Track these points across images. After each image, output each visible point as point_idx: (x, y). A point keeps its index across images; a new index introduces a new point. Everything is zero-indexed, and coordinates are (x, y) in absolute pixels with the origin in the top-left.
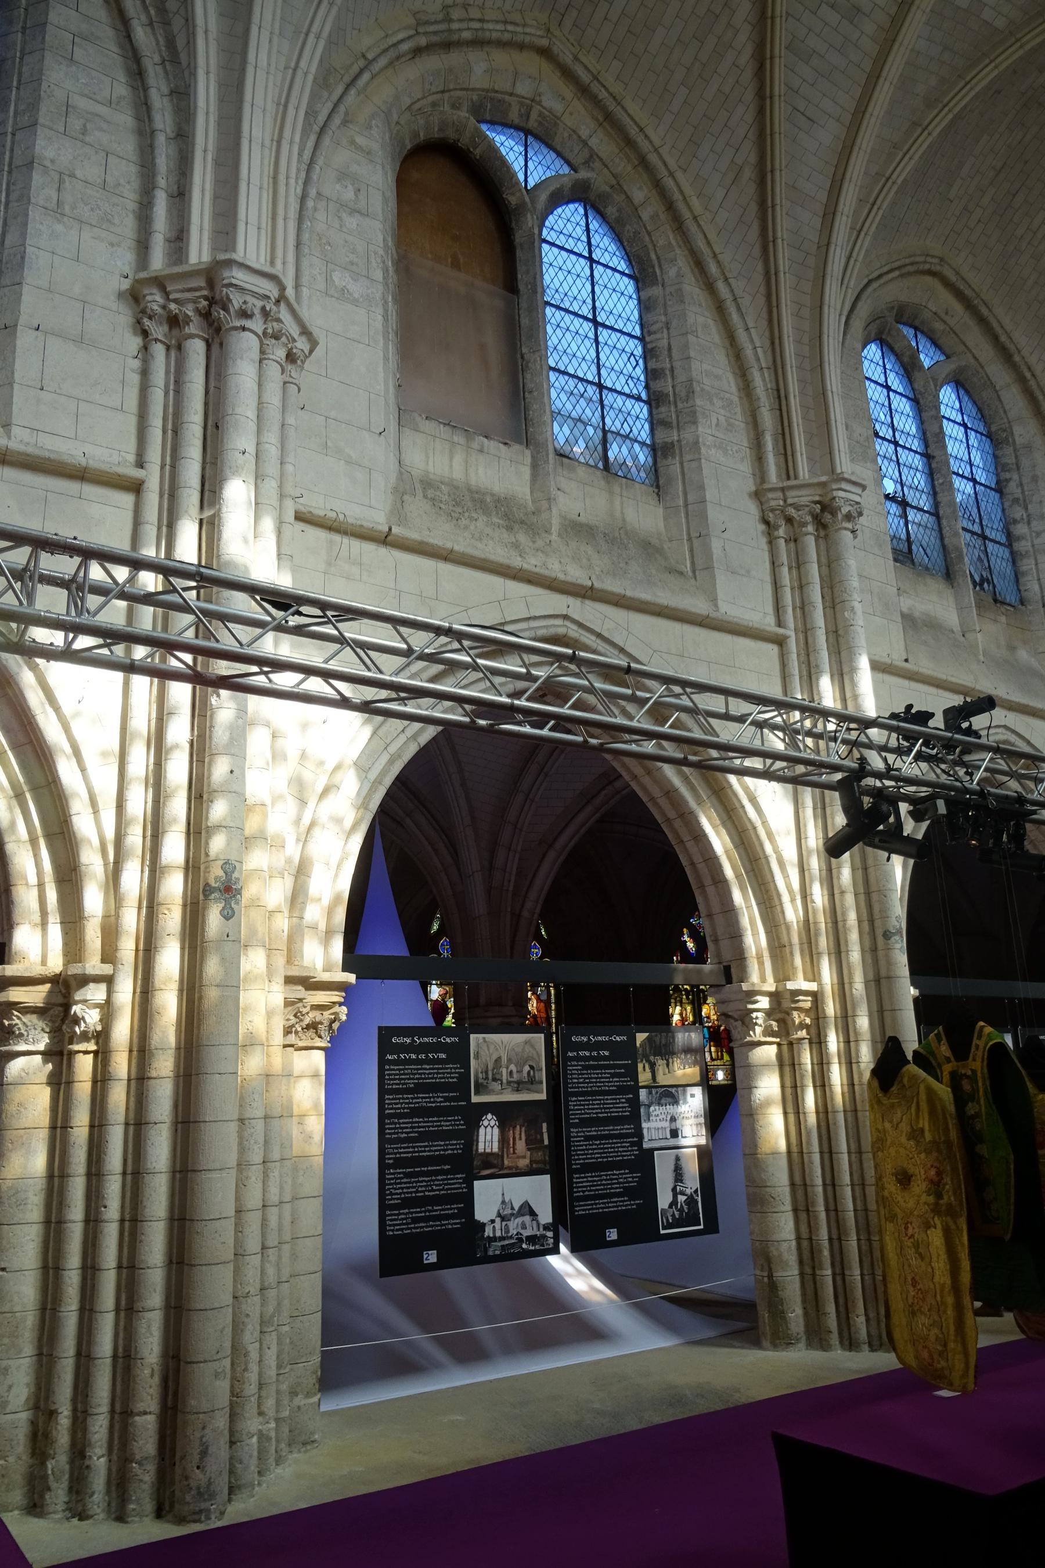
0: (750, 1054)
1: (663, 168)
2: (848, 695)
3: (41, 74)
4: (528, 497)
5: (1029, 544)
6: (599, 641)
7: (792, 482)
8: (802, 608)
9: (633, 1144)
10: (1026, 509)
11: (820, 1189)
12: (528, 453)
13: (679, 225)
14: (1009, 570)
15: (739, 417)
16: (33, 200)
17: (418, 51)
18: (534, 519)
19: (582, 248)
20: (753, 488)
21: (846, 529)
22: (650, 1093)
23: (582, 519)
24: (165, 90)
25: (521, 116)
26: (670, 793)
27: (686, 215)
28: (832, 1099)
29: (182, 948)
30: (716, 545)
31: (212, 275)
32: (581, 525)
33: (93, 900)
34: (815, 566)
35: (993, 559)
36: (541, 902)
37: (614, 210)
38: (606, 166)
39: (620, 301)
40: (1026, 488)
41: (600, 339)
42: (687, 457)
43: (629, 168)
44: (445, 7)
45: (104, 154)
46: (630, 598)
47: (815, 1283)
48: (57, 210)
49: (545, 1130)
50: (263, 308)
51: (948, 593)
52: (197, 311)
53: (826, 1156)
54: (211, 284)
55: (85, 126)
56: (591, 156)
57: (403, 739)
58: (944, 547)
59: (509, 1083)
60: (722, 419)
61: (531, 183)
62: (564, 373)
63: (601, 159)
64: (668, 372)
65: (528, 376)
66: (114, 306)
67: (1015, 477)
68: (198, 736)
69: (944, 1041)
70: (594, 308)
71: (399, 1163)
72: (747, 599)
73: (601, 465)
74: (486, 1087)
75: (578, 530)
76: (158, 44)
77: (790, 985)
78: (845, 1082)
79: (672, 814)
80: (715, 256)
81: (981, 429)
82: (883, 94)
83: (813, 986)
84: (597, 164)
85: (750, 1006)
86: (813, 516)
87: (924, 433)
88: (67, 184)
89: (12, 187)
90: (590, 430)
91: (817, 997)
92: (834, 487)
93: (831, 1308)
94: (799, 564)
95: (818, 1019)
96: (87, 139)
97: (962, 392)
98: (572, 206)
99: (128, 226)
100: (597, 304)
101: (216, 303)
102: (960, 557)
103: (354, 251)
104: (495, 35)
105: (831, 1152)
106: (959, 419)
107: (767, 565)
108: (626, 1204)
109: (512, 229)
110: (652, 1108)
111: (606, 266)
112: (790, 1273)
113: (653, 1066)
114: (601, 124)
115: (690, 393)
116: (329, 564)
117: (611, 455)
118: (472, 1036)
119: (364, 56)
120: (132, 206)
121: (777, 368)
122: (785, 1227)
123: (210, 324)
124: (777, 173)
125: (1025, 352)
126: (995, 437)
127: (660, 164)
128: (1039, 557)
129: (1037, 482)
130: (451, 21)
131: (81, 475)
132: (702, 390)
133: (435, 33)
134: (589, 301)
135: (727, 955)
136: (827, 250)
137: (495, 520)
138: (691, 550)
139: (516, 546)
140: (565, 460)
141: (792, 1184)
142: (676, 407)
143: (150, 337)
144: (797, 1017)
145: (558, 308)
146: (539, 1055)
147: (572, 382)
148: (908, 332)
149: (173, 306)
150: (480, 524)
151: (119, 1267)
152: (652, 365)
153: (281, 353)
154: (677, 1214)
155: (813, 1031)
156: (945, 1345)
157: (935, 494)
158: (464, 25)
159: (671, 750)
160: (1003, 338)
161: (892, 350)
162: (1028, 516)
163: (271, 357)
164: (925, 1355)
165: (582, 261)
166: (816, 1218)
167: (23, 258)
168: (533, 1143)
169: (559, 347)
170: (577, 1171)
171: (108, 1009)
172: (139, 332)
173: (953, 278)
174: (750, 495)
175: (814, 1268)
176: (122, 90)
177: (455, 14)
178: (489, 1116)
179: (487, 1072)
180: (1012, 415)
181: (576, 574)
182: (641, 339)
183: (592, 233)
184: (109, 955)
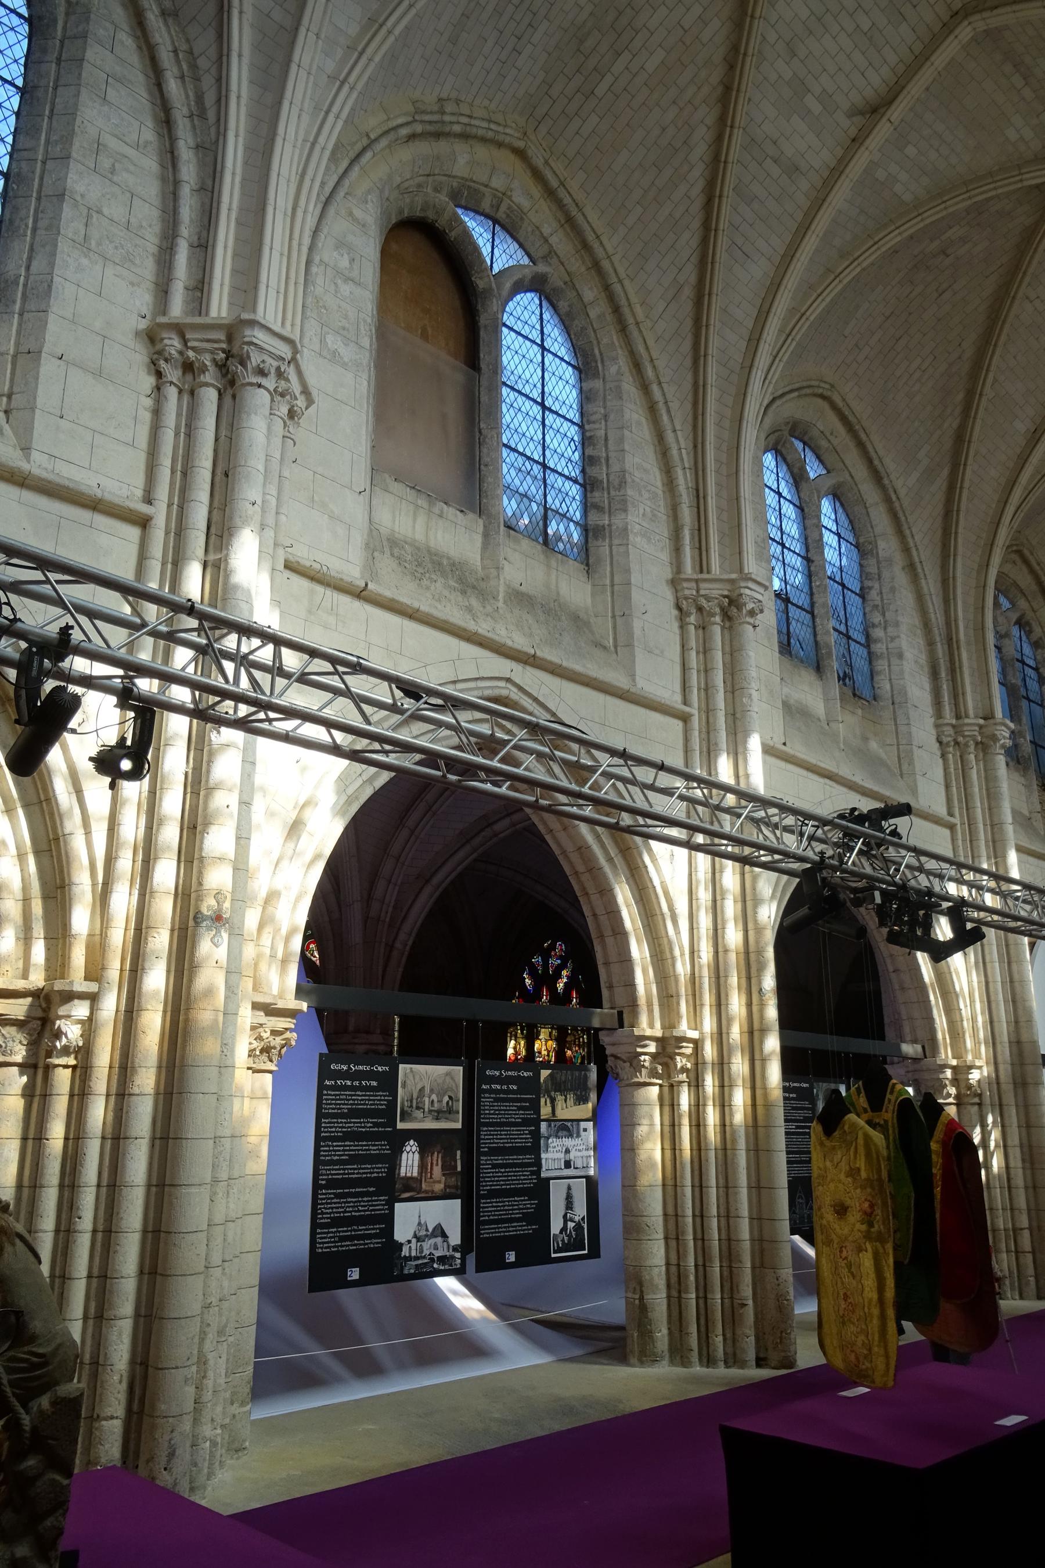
0: (635, 1093)
1: (613, 275)
2: (741, 773)
3: (77, 109)
4: (479, 564)
6: (534, 704)
7: (705, 576)
8: (706, 690)
9: (532, 1173)
10: (884, 615)
11: (690, 1220)
12: (481, 522)
13: (623, 329)
14: (866, 668)
15: (662, 509)
16: (62, 231)
17: (412, 137)
18: (483, 585)
19: (535, 335)
20: (670, 576)
21: (749, 623)
22: (550, 1126)
23: (523, 589)
24: (191, 142)
25: (492, 206)
26: (583, 849)
27: (631, 320)
28: (706, 1137)
29: (168, 971)
30: (637, 625)
31: (232, 331)
32: (523, 594)
33: (81, 919)
34: (720, 653)
35: (854, 657)
36: (414, 935)
37: (566, 304)
38: (562, 264)
41: (547, 422)
42: (616, 542)
43: (583, 269)
44: (440, 100)
45: (129, 195)
46: (565, 668)
47: (680, 1306)
48: (84, 244)
49: (458, 1157)
50: (278, 369)
51: (818, 684)
52: (214, 360)
53: (697, 1190)
54: (230, 339)
55: (113, 165)
56: (550, 252)
57: (360, 782)
58: (816, 642)
59: (430, 1111)
60: (648, 509)
61: (496, 269)
62: (515, 450)
63: (558, 257)
64: (603, 461)
65: (485, 450)
66: (131, 344)
67: (877, 586)
68: (194, 769)
69: (863, 1094)
70: (543, 392)
71: (332, 1184)
72: (659, 675)
73: (541, 540)
74: (410, 1115)
75: (520, 598)
76: (187, 97)
77: (676, 1033)
78: (718, 1123)
79: (581, 868)
80: (652, 360)
81: (851, 539)
82: (811, 243)
83: (694, 1034)
84: (555, 260)
85: (639, 1050)
86: (722, 609)
87: (806, 539)
88: (94, 219)
89: (40, 215)
90: (534, 506)
91: (697, 1044)
92: (743, 584)
93: (693, 1329)
94: (705, 650)
95: (697, 1064)
96: (115, 179)
97: (838, 504)
98: (529, 295)
99: (148, 269)
100: (546, 389)
101: (232, 356)
102: (830, 654)
103: (346, 317)
104: (480, 132)
105: (701, 1186)
106: (834, 529)
107: (678, 648)
108: (525, 1229)
109: (478, 311)
110: (550, 1140)
111: (555, 355)
112: (658, 1296)
113: (553, 1101)
114: (562, 226)
115: (623, 483)
116: (310, 612)
117: (550, 531)
118: (401, 1066)
119: (368, 135)
120: (153, 249)
121: (698, 470)
122: (656, 1254)
123: (224, 375)
124: (714, 297)
125: (892, 477)
126: (863, 549)
127: (611, 271)
130: (443, 113)
131: (95, 505)
132: (633, 481)
133: (430, 122)
134: (539, 385)
135: (621, 1001)
136: (750, 372)
137: (452, 583)
138: (615, 628)
139: (469, 609)
140: (512, 532)
141: (665, 1215)
142: (609, 493)
143: (164, 379)
144: (680, 1062)
145: (512, 388)
146: (457, 1087)
147: (520, 459)
148: (799, 445)
149: (191, 354)
150: (438, 584)
151: (89, 1277)
152: (589, 451)
153: (284, 410)
154: (566, 1239)
155: (692, 1075)
156: (870, 1350)
157: (812, 594)
158: (453, 119)
159: (588, 811)
160: (876, 462)
161: (785, 460)
162: (886, 622)
163: (277, 413)
164: (852, 1357)
165: (535, 347)
166: (685, 1246)
167: (50, 287)
168: (448, 1168)
169: (512, 426)
170: (484, 1197)
171: (90, 1025)
172: (153, 372)
173: (840, 404)
174: (667, 581)
175: (680, 1292)
176: (149, 134)
177: (449, 108)
178: (412, 1142)
179: (411, 1101)
180: (878, 530)
181: (519, 641)
182: (581, 427)
183: (545, 322)
184: (95, 972)
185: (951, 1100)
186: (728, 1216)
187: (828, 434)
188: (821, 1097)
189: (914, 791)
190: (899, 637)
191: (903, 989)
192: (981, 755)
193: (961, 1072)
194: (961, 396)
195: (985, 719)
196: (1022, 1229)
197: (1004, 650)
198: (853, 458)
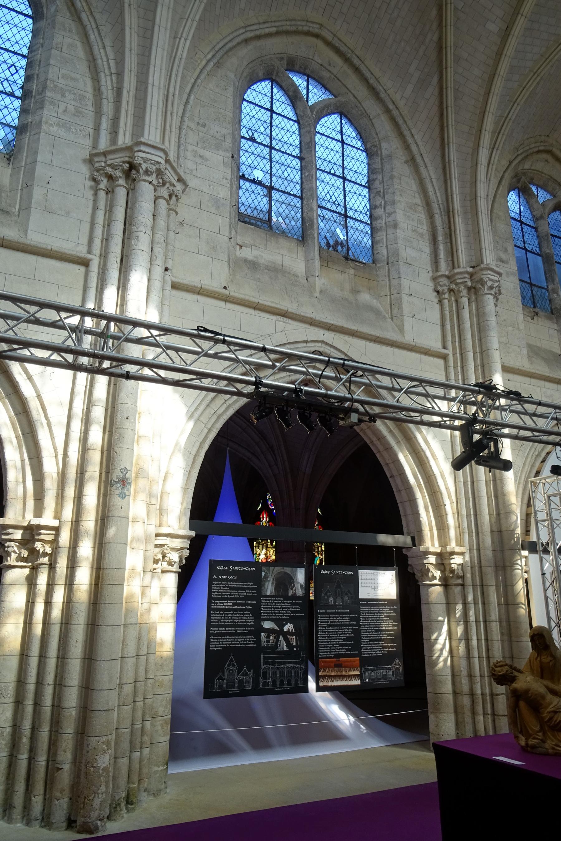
5: (384, 221)
10: (384, 198)
39: (358, 163)
40: (385, 184)
85: (4, 537)
91: (57, 530)
128: (388, 230)
129: (393, 179)
132: (56, 86)
173: (329, 37)
180: (381, 136)
185: (436, 582)
186: (60, 684)
187: (328, 67)
188: (270, 578)
189: (401, 329)
190: (395, 212)
191: (399, 491)
192: (473, 297)
193: (443, 559)
194: (434, 12)
195: (473, 267)
196: (497, 695)
197: (539, 229)
198: (352, 81)
